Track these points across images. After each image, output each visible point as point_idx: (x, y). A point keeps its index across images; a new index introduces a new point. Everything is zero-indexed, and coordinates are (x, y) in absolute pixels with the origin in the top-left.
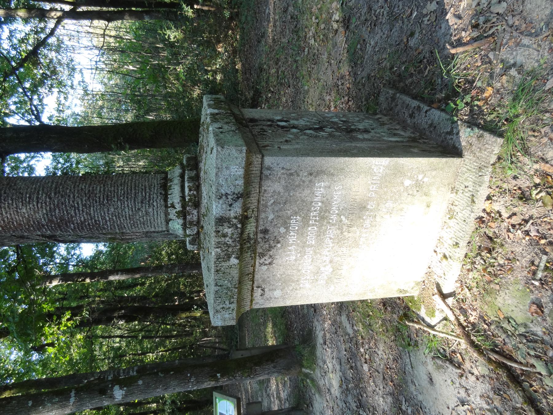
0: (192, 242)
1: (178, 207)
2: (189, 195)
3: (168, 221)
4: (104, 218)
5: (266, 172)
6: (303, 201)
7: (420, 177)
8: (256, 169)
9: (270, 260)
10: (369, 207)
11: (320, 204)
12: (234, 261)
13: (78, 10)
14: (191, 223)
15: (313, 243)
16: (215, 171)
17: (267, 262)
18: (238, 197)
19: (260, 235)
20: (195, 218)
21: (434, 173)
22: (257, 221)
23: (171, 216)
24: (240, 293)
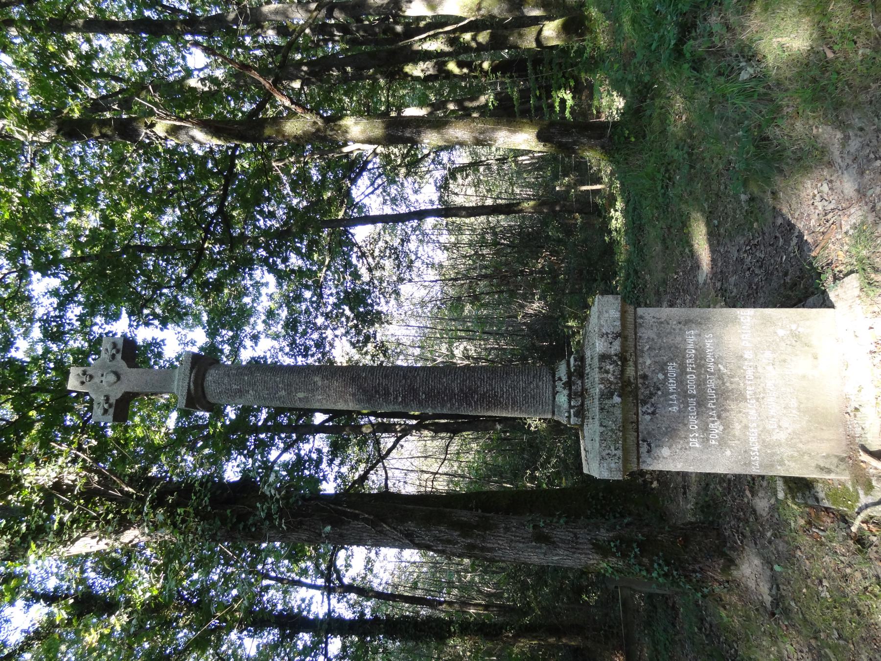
1: (565, 379)
2: (574, 366)
3: (555, 393)
4: (502, 390)
5: (640, 321)
6: (676, 348)
7: (794, 327)
8: (630, 318)
9: (652, 409)
11: (694, 351)
12: (617, 399)
14: (576, 394)
15: (695, 393)
18: (617, 336)
19: (640, 381)
20: (580, 389)
22: (636, 364)
23: (558, 389)
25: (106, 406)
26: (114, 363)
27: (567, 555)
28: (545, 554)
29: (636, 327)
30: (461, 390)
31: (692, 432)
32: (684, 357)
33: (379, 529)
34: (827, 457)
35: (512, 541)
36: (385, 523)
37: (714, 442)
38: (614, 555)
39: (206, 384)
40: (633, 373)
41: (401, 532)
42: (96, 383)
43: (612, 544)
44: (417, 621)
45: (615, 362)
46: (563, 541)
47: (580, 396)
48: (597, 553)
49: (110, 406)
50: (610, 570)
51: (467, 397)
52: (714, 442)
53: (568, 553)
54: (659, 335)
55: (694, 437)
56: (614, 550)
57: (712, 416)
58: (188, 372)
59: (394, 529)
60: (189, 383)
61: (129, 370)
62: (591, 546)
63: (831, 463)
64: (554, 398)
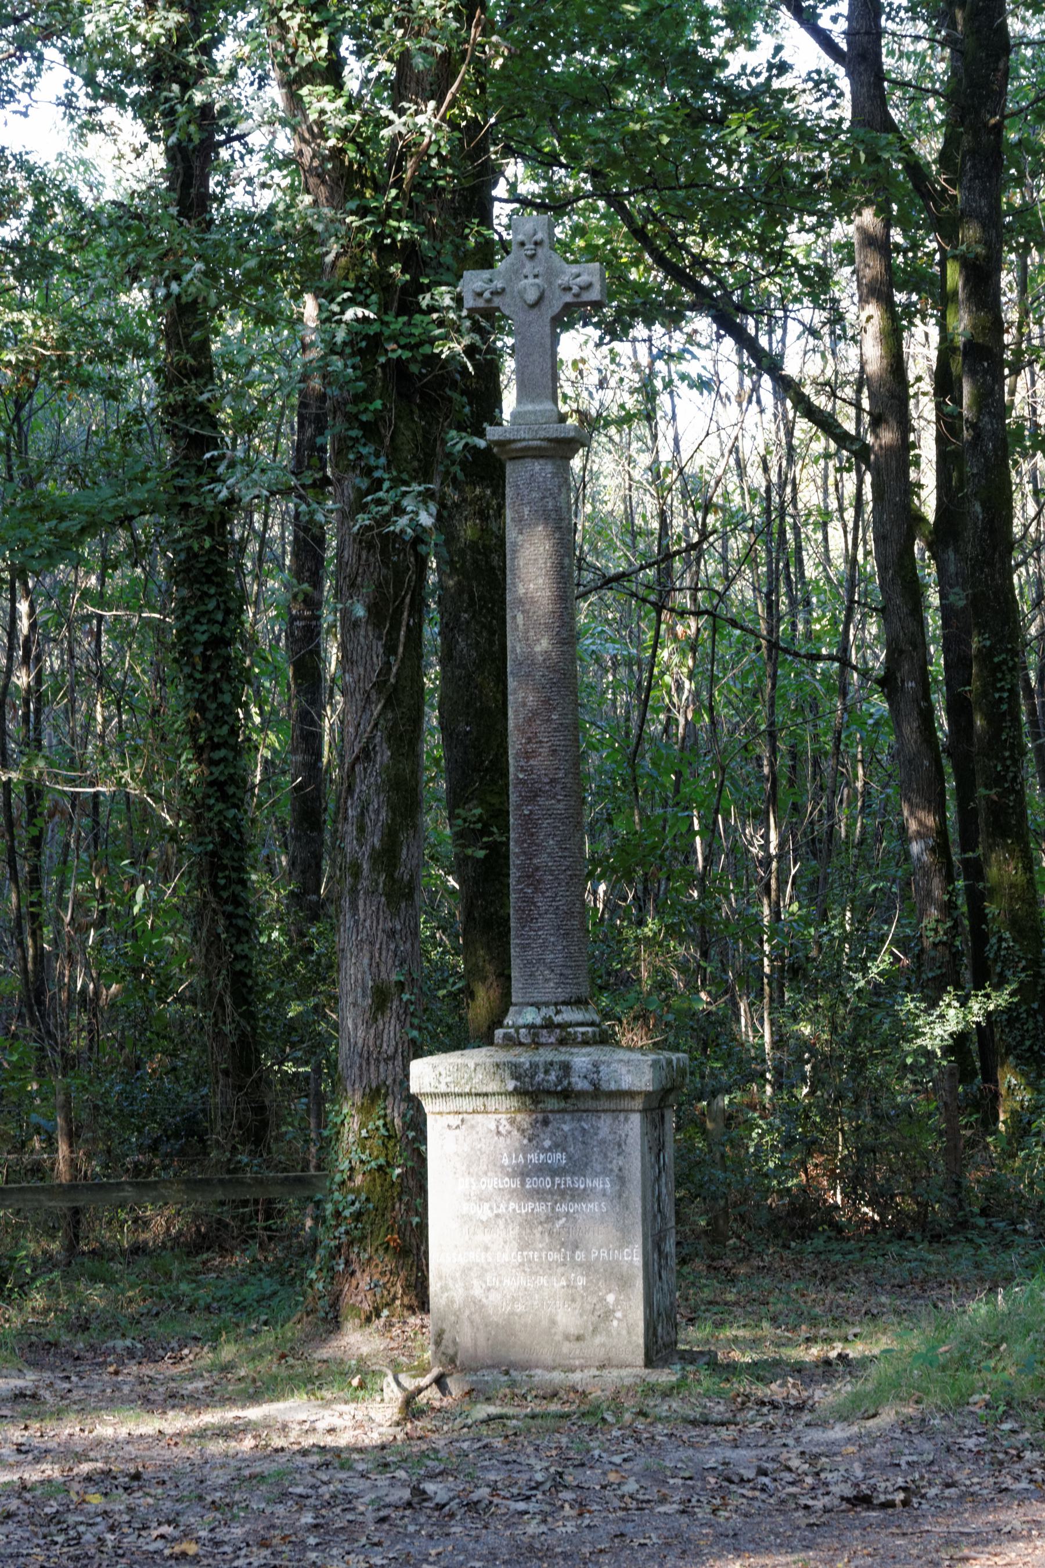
0: (507, 1037)
1: (558, 1019)
3: (537, 1005)
5: (622, 1117)
7: (619, 1314)
8: (626, 1103)
13: (931, 517)
14: (536, 1035)
19: (540, 1116)
20: (543, 1040)
22: (563, 1111)
23: (544, 1010)
24: (460, 1095)
25: (487, 295)
26: (558, 292)
30: (537, 869)
33: (374, 697)
34: (455, 1342)
35: (372, 944)
36: (384, 707)
38: (363, 1125)
41: (371, 739)
42: (523, 266)
44: (228, 643)
45: (560, 1082)
46: (378, 1036)
49: (489, 301)
50: (338, 1120)
54: (602, 1142)
56: (371, 1126)
58: (542, 434)
59: (376, 725)
61: (547, 319)
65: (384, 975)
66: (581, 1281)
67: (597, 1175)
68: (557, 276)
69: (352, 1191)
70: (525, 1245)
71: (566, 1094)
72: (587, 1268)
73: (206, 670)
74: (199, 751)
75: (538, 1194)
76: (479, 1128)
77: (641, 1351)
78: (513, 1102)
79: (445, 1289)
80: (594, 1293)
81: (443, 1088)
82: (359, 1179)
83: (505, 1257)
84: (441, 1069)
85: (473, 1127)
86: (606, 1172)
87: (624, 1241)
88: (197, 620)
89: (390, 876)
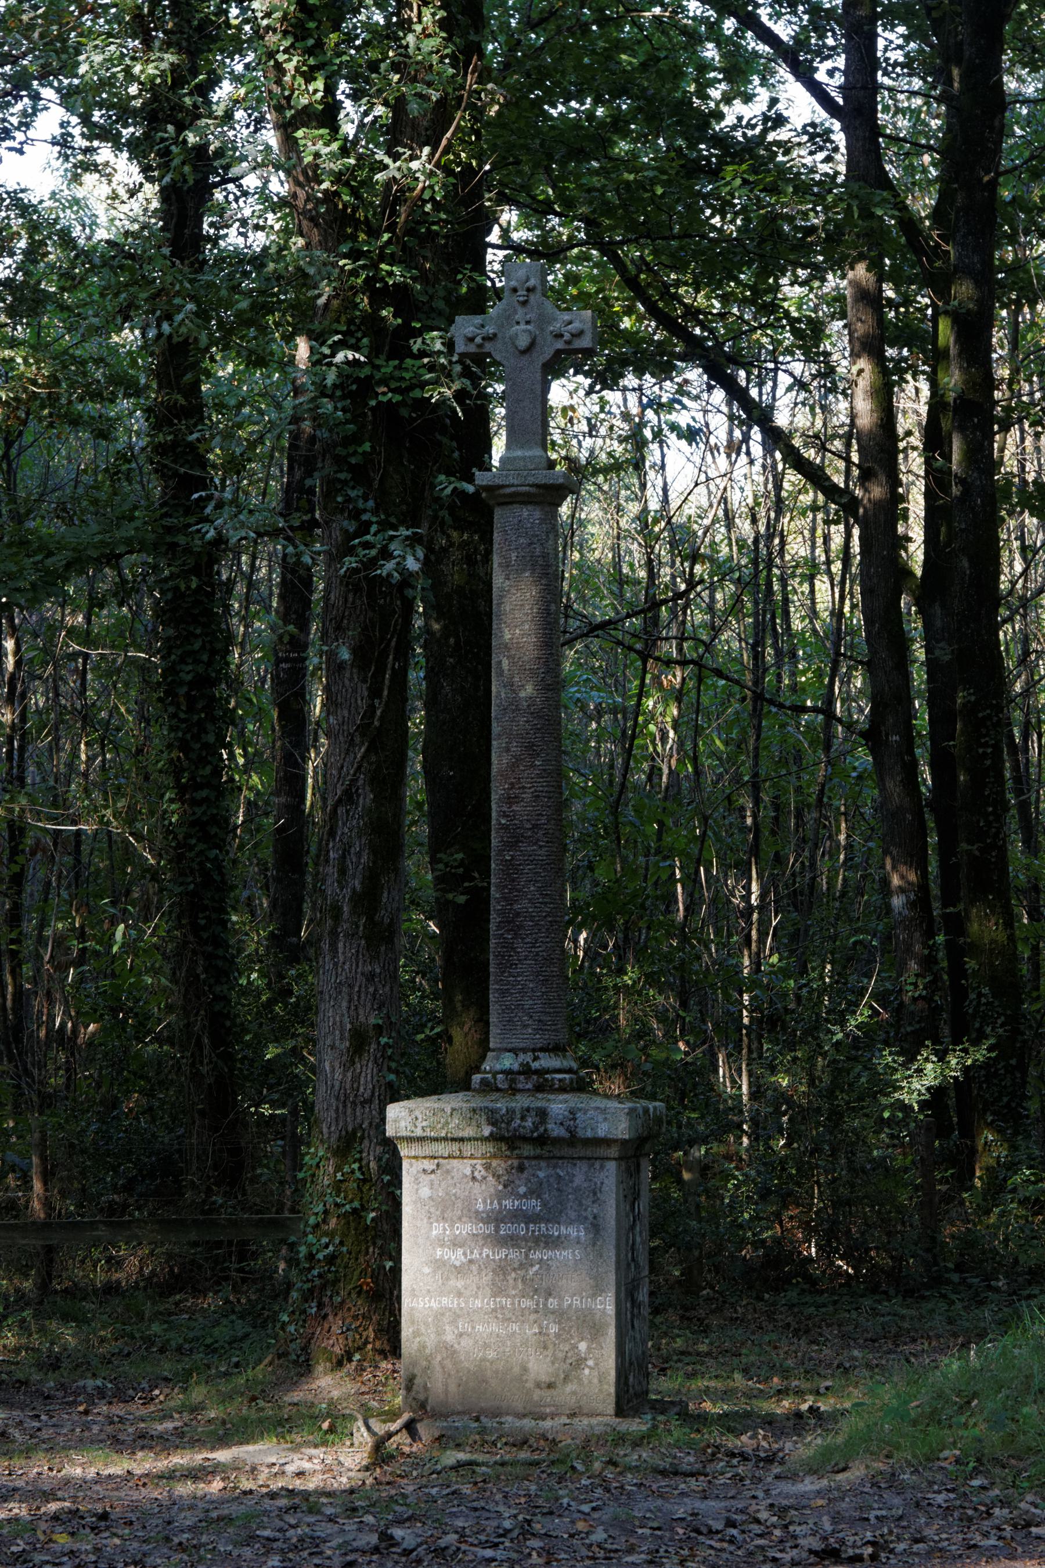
1: (535, 1065)
3: (515, 1051)
5: (597, 1165)
6: (561, 1212)
7: (590, 1363)
8: (602, 1152)
9: (479, 1177)
10: (551, 1300)
13: (919, 572)
14: (513, 1081)
16: (602, 1106)
17: (476, 1174)
19: (516, 1163)
20: (520, 1086)
21: (596, 1381)
23: (522, 1056)
24: (436, 1139)
25: (478, 340)
26: (549, 338)
27: (333, 1086)
28: (333, 1047)
29: (589, 1159)
30: (518, 915)
31: (452, 1226)
32: (548, 1221)
33: (357, 739)
34: (425, 1388)
36: (367, 751)
37: (439, 1253)
38: (338, 1168)
39: (516, 507)
40: (526, 1154)
42: (515, 312)
43: (356, 1166)
44: (214, 683)
45: (536, 1128)
46: (356, 1079)
47: (510, 1087)
48: (340, 1139)
49: (480, 346)
50: (314, 1162)
51: (509, 922)
52: (439, 1253)
53: (337, 1088)
54: (577, 1190)
55: (445, 1229)
56: (346, 1169)
57: (472, 1253)
58: (531, 480)
59: (359, 768)
60: (513, 485)
62: (350, 1129)
63: (418, 1392)
64: (509, 1051)
65: (362, 1018)
66: (554, 1329)
67: (571, 1222)
68: (549, 323)
69: (326, 1234)
70: (498, 1291)
71: (543, 1140)
72: (560, 1315)
73: (190, 709)
74: (182, 791)
75: (511, 1241)
76: (454, 1173)
77: (612, 1400)
78: (489, 1148)
79: (417, 1334)
80: (566, 1340)
81: (419, 1132)
82: (333, 1222)
83: (478, 1303)
84: (417, 1113)
85: (448, 1172)
86: (581, 1219)
87: (598, 1290)
88: (182, 660)
89: (371, 919)
